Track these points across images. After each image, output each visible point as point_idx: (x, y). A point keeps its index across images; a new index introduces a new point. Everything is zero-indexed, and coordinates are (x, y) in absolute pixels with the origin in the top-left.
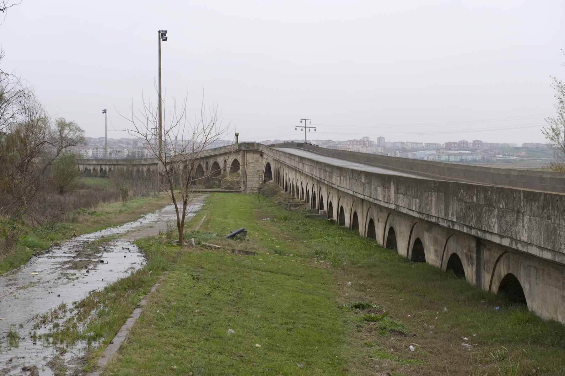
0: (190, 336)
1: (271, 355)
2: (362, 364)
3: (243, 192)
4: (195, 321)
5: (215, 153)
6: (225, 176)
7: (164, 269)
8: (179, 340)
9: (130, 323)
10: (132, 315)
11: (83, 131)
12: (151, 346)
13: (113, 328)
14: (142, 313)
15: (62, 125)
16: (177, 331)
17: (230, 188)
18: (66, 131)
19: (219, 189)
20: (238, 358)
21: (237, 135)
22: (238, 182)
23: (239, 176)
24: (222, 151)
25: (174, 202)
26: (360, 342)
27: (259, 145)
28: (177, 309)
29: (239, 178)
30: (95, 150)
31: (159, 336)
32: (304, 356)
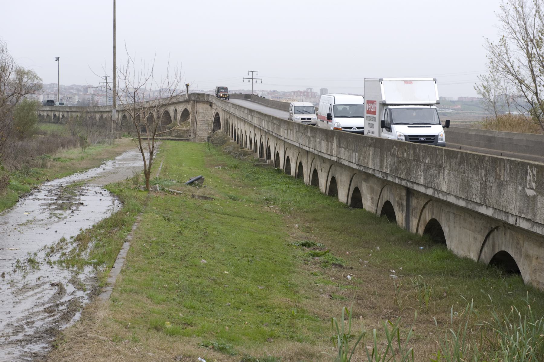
0: (173, 264)
1: (238, 280)
2: (309, 288)
3: (192, 140)
4: (174, 253)
5: (167, 102)
7: (139, 211)
8: (165, 267)
9: (123, 253)
10: (123, 247)
11: (41, 79)
12: (144, 271)
13: (111, 257)
14: (131, 246)
15: (20, 73)
16: (161, 260)
17: (180, 136)
18: (25, 80)
19: (169, 137)
20: (212, 281)
21: (187, 86)
22: (188, 131)
23: (189, 125)
24: (173, 100)
25: (142, 152)
26: (307, 272)
27: (208, 95)
28: (157, 244)
30: (47, 96)
31: (149, 263)
32: (264, 281)
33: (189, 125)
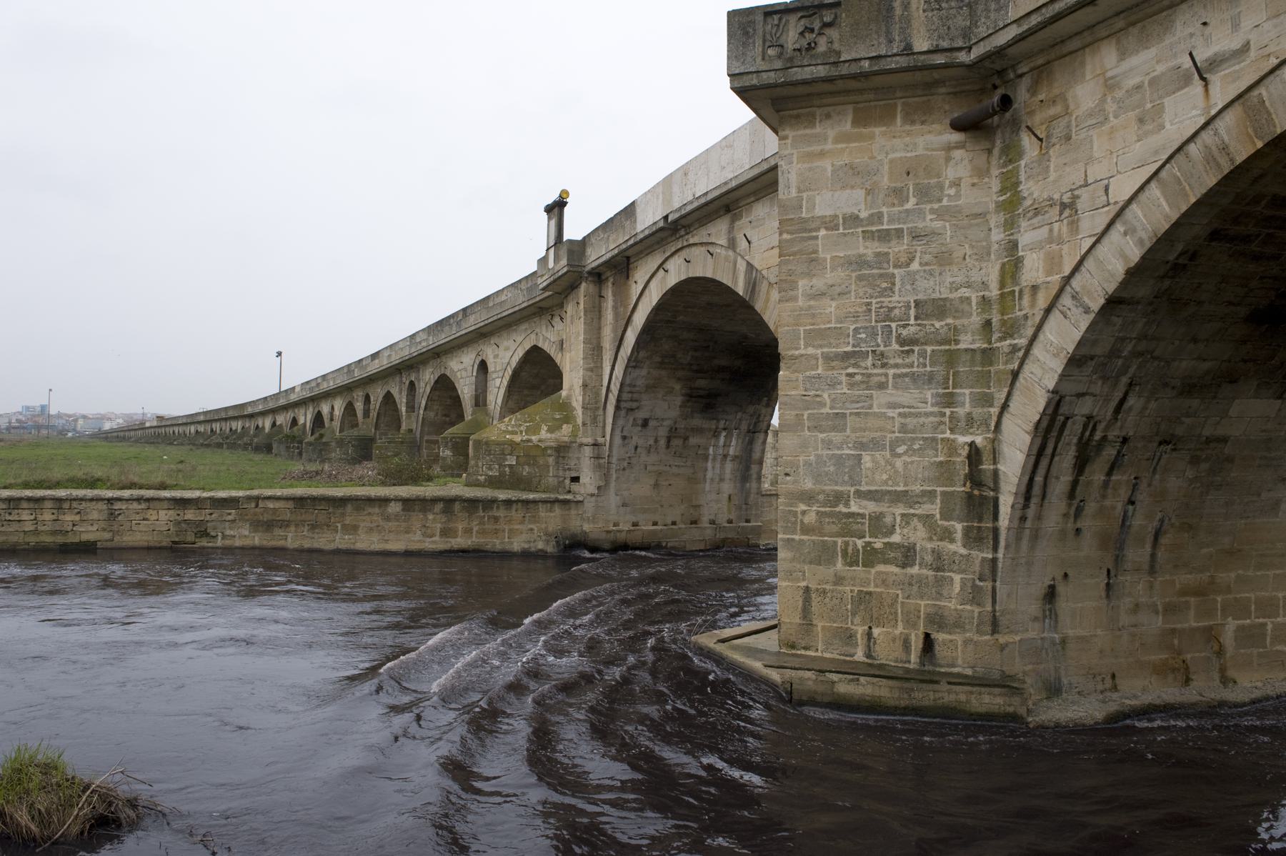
3: (589, 505)
6: (478, 426)
19: (456, 488)
21: (556, 208)
22: (562, 450)
24: (472, 323)
29: (566, 429)
33: (568, 419)
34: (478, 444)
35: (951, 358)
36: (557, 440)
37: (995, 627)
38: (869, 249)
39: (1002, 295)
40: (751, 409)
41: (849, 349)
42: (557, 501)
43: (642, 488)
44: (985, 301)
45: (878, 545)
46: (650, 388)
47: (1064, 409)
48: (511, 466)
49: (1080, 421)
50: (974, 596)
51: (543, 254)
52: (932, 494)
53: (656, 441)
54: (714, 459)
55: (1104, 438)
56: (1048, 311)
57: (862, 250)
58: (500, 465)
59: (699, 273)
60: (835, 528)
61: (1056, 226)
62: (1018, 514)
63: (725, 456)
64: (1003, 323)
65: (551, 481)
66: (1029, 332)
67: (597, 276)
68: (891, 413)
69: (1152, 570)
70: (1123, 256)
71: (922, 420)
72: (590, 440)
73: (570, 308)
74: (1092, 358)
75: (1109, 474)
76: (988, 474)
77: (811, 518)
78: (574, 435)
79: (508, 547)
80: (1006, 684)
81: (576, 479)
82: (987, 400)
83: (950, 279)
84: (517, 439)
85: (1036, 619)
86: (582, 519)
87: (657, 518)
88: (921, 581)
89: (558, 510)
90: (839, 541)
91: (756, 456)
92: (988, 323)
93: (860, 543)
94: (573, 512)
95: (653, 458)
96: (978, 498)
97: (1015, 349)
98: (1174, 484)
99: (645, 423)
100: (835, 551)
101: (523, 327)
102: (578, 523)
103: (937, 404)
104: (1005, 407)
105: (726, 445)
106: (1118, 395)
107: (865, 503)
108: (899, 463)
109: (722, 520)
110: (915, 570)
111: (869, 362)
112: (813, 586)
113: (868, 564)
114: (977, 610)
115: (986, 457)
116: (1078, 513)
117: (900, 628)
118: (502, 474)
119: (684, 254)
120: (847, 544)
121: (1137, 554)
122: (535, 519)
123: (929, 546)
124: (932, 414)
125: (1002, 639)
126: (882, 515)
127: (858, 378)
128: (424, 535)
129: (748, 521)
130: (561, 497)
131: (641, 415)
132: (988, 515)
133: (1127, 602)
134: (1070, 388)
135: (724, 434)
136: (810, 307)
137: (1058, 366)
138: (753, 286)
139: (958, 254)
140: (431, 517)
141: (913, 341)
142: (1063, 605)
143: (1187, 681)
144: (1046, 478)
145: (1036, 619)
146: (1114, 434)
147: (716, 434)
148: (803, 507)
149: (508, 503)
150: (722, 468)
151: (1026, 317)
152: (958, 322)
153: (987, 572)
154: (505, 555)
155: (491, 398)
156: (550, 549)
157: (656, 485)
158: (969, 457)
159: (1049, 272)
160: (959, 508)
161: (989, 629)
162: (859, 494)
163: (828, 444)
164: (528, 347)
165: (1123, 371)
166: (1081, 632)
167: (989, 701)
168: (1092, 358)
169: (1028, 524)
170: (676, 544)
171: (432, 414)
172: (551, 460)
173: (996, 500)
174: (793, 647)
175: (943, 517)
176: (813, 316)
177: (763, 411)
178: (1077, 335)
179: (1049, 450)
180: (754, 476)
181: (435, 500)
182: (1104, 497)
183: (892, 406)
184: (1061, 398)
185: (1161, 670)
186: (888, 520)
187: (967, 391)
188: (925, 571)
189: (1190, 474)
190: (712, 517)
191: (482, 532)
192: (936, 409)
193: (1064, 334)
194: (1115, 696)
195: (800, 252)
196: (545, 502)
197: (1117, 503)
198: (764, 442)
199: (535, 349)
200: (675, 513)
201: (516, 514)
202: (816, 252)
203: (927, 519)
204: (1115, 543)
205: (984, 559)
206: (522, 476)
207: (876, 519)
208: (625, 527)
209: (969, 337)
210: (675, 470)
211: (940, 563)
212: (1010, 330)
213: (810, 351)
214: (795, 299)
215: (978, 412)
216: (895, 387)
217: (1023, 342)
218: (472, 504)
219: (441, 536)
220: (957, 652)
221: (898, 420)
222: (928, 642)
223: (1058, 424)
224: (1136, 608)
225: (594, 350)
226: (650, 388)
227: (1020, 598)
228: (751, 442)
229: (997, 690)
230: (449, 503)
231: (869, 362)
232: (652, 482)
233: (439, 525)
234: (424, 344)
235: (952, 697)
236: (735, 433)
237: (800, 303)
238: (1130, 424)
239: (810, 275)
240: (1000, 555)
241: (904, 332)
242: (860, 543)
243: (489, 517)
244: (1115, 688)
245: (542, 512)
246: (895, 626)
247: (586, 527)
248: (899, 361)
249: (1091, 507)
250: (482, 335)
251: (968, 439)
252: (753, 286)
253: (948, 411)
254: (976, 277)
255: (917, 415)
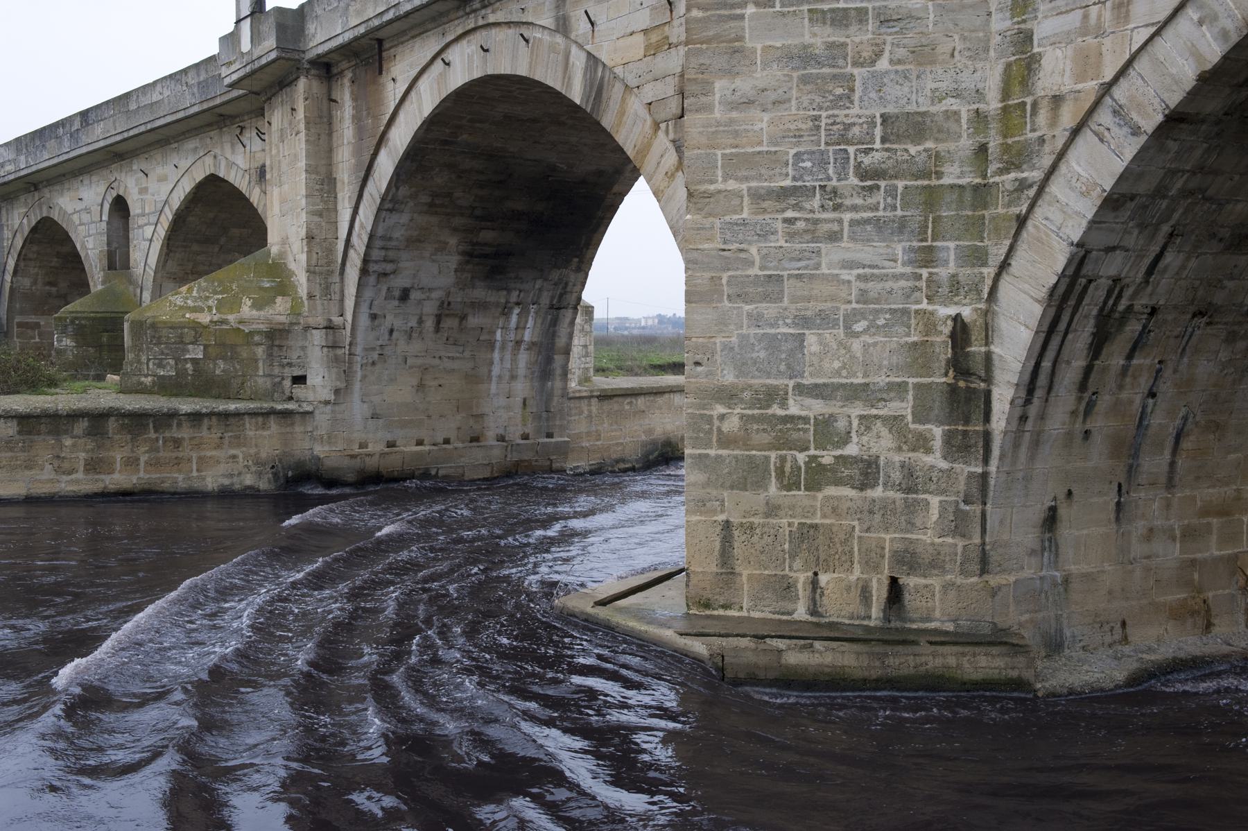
3: (323, 418)
17: (204, 385)
19: (104, 395)
22: (276, 336)
24: (99, 136)
33: (284, 287)
34: (138, 327)
35: (931, 198)
36: (269, 321)
37: (984, 566)
38: (818, 37)
39: (1005, 110)
40: (555, 275)
41: (788, 183)
42: (272, 412)
43: (400, 391)
44: (979, 118)
45: (827, 458)
46: (413, 242)
47: (1088, 269)
48: (195, 361)
49: (1104, 283)
50: (957, 523)
51: (230, 28)
52: (901, 388)
53: (420, 321)
54: (503, 348)
55: (1130, 308)
56: (1076, 132)
57: (807, 39)
58: (177, 360)
59: (504, 68)
60: (766, 438)
61: (1094, 11)
62: (1018, 412)
63: (518, 343)
64: (1006, 148)
65: (262, 382)
66: (1047, 161)
67: (326, 68)
68: (846, 275)
69: (1170, 485)
70: (1196, 55)
71: (889, 285)
72: (320, 320)
73: (277, 118)
74: (1132, 198)
75: (1130, 357)
76: (980, 359)
77: (732, 425)
78: (295, 311)
79: (197, 485)
80: (999, 639)
81: (300, 380)
82: (978, 257)
83: (931, 85)
84: (205, 318)
85: (1033, 552)
86: (313, 439)
87: (423, 434)
88: (886, 507)
89: (274, 426)
90: (773, 455)
91: (561, 342)
92: (982, 149)
93: (801, 458)
94: (298, 429)
95: (416, 346)
96: (964, 394)
97: (1022, 185)
98: (1205, 369)
99: (405, 295)
100: (767, 471)
101: (191, 144)
102: (307, 445)
103: (910, 262)
104: (1004, 266)
105: (520, 327)
106: (1155, 249)
107: (809, 401)
108: (856, 345)
109: (514, 435)
110: (878, 492)
111: (816, 202)
112: (735, 520)
113: (813, 486)
114: (961, 544)
115: (976, 335)
116: (1088, 412)
117: (857, 573)
118: (181, 373)
119: (478, 38)
120: (783, 459)
121: (1154, 463)
122: (239, 441)
123: (897, 458)
124: (902, 276)
125: (994, 580)
126: (832, 418)
127: (801, 225)
128: (58, 470)
129: (550, 435)
130: (279, 407)
131: (400, 282)
132: (978, 415)
133: (1140, 526)
134: (1101, 239)
135: (517, 311)
136: (732, 121)
137: (1088, 208)
138: (597, 90)
139: (944, 48)
140: (68, 442)
141: (878, 174)
142: (1066, 532)
143: (1208, 626)
144: (1055, 363)
145: (1033, 552)
146: (1142, 302)
147: (506, 311)
148: (721, 409)
149: (196, 417)
150: (514, 360)
151: (1041, 140)
152: (941, 147)
153: (975, 491)
154: (194, 497)
155: (136, 256)
156: (264, 485)
157: (421, 387)
158: (953, 335)
159: (1080, 77)
160: (938, 405)
161: (976, 567)
162: (800, 390)
163: (757, 320)
164: (199, 176)
165: (1165, 218)
166: (1085, 568)
167: (984, 665)
168: (1132, 198)
169: (1029, 426)
170: (451, 472)
171: (26, 282)
172: (260, 351)
173: (988, 395)
174: (707, 605)
175: (918, 419)
176: (736, 134)
177: (572, 277)
178: (1119, 166)
179: (1062, 326)
180: (558, 371)
181: (75, 416)
182: (1121, 387)
183: (849, 265)
184: (1088, 252)
185: (1179, 614)
186: (841, 424)
187: (952, 245)
188: (891, 494)
189: (1223, 356)
190: (501, 431)
191: (155, 464)
192: (908, 270)
193: (1098, 165)
194: (1127, 649)
195: (717, 38)
196: (253, 414)
197: (1134, 396)
198: (572, 323)
199: (213, 181)
200: (448, 427)
201: (208, 433)
202: (740, 38)
203: (894, 422)
204: (1129, 450)
205: (971, 475)
206: (213, 378)
207: (824, 426)
208: (376, 447)
209: (955, 169)
210: (449, 364)
211: (911, 482)
212: (1016, 158)
213: (732, 185)
214: (709, 108)
215: (966, 273)
216: (852, 238)
217: (1036, 175)
218: (136, 421)
219: (87, 471)
220: (936, 601)
221: (857, 285)
222: (895, 590)
223: (1078, 288)
224: (1150, 533)
225: (323, 183)
226: (413, 242)
227: (1014, 525)
228: (555, 322)
229: (995, 650)
230: (97, 420)
231: (816, 202)
232: (415, 382)
233: (82, 455)
234: (9, 168)
235: (939, 662)
236: (533, 308)
237: (717, 114)
238: (1163, 289)
239: (731, 73)
240: (993, 468)
241: (867, 160)
242: (801, 458)
243: (165, 441)
244: (1125, 640)
245: (250, 429)
246: (850, 570)
247: (320, 450)
248: (859, 201)
249: (1105, 401)
250: (117, 155)
251: (952, 311)
252: (597, 90)
253: (925, 273)
254: (968, 81)
255: (883, 278)
